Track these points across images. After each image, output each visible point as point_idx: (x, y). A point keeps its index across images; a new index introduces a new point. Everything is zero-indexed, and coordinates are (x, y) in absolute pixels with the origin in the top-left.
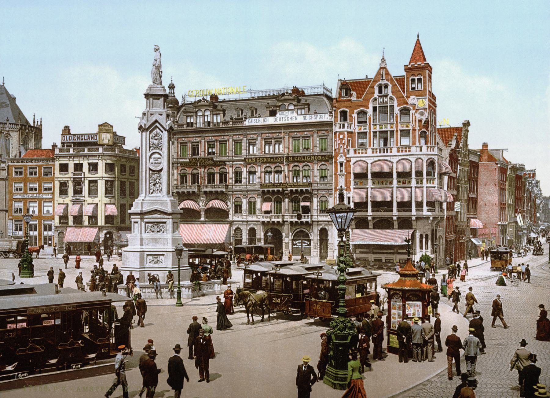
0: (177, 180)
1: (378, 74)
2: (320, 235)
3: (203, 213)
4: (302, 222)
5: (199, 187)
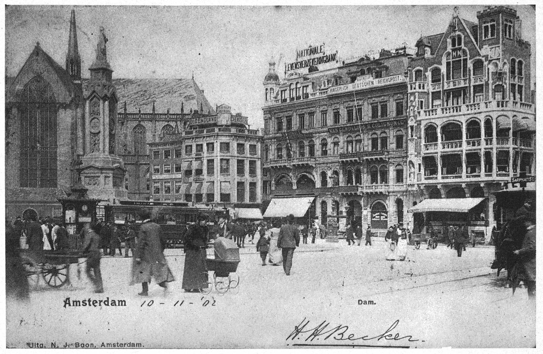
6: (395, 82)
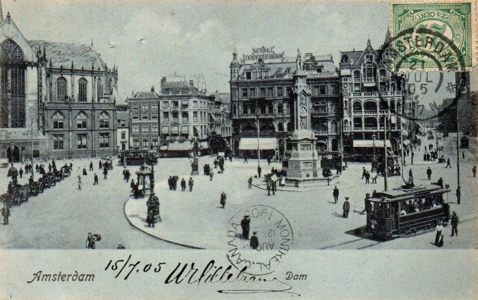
1: (367, 49)
6: (332, 76)
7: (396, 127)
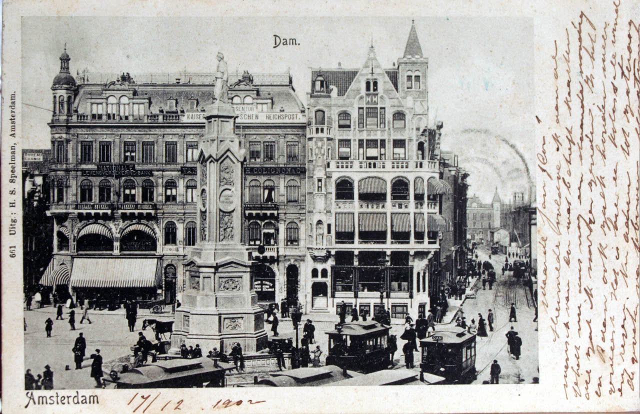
0: (76, 195)
2: (288, 275)
3: (117, 244)
4: (265, 257)
5: (112, 207)
7: (426, 239)
